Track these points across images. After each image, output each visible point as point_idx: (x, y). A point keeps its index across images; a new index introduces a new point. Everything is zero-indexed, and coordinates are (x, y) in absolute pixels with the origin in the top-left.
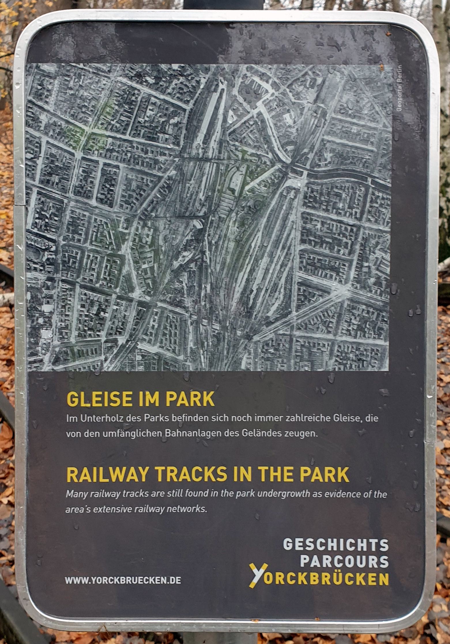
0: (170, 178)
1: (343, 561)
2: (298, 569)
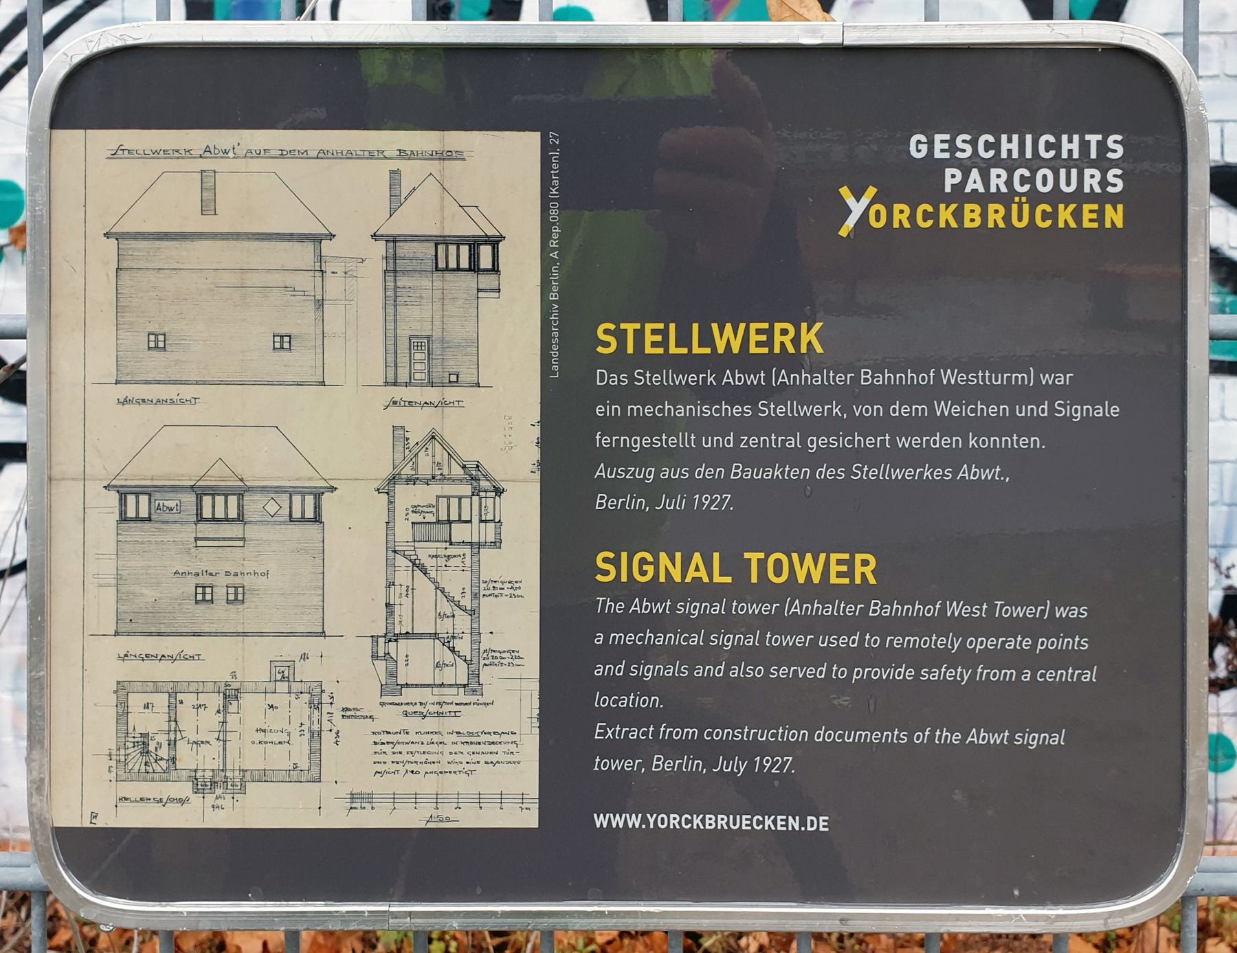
1: (1031, 180)
2: (937, 196)
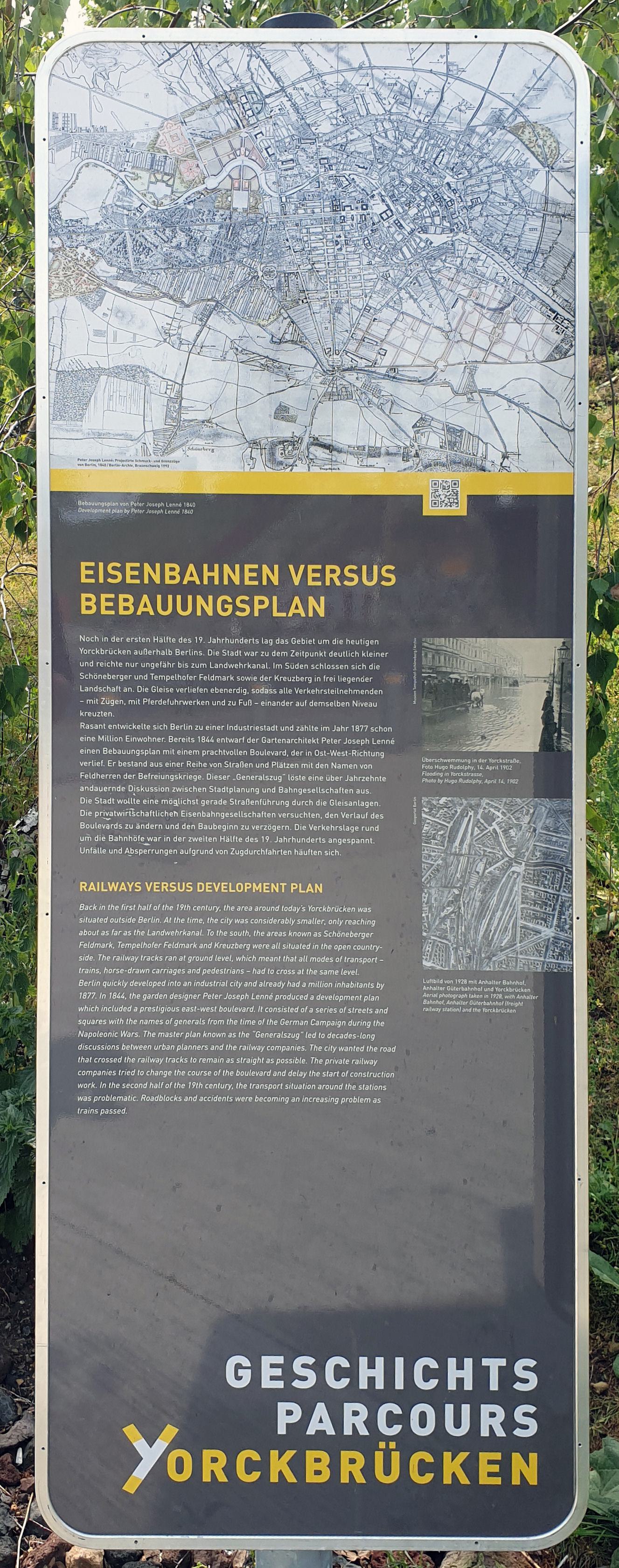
0: (438, 865)
1: (404, 1419)
2: (267, 1440)
